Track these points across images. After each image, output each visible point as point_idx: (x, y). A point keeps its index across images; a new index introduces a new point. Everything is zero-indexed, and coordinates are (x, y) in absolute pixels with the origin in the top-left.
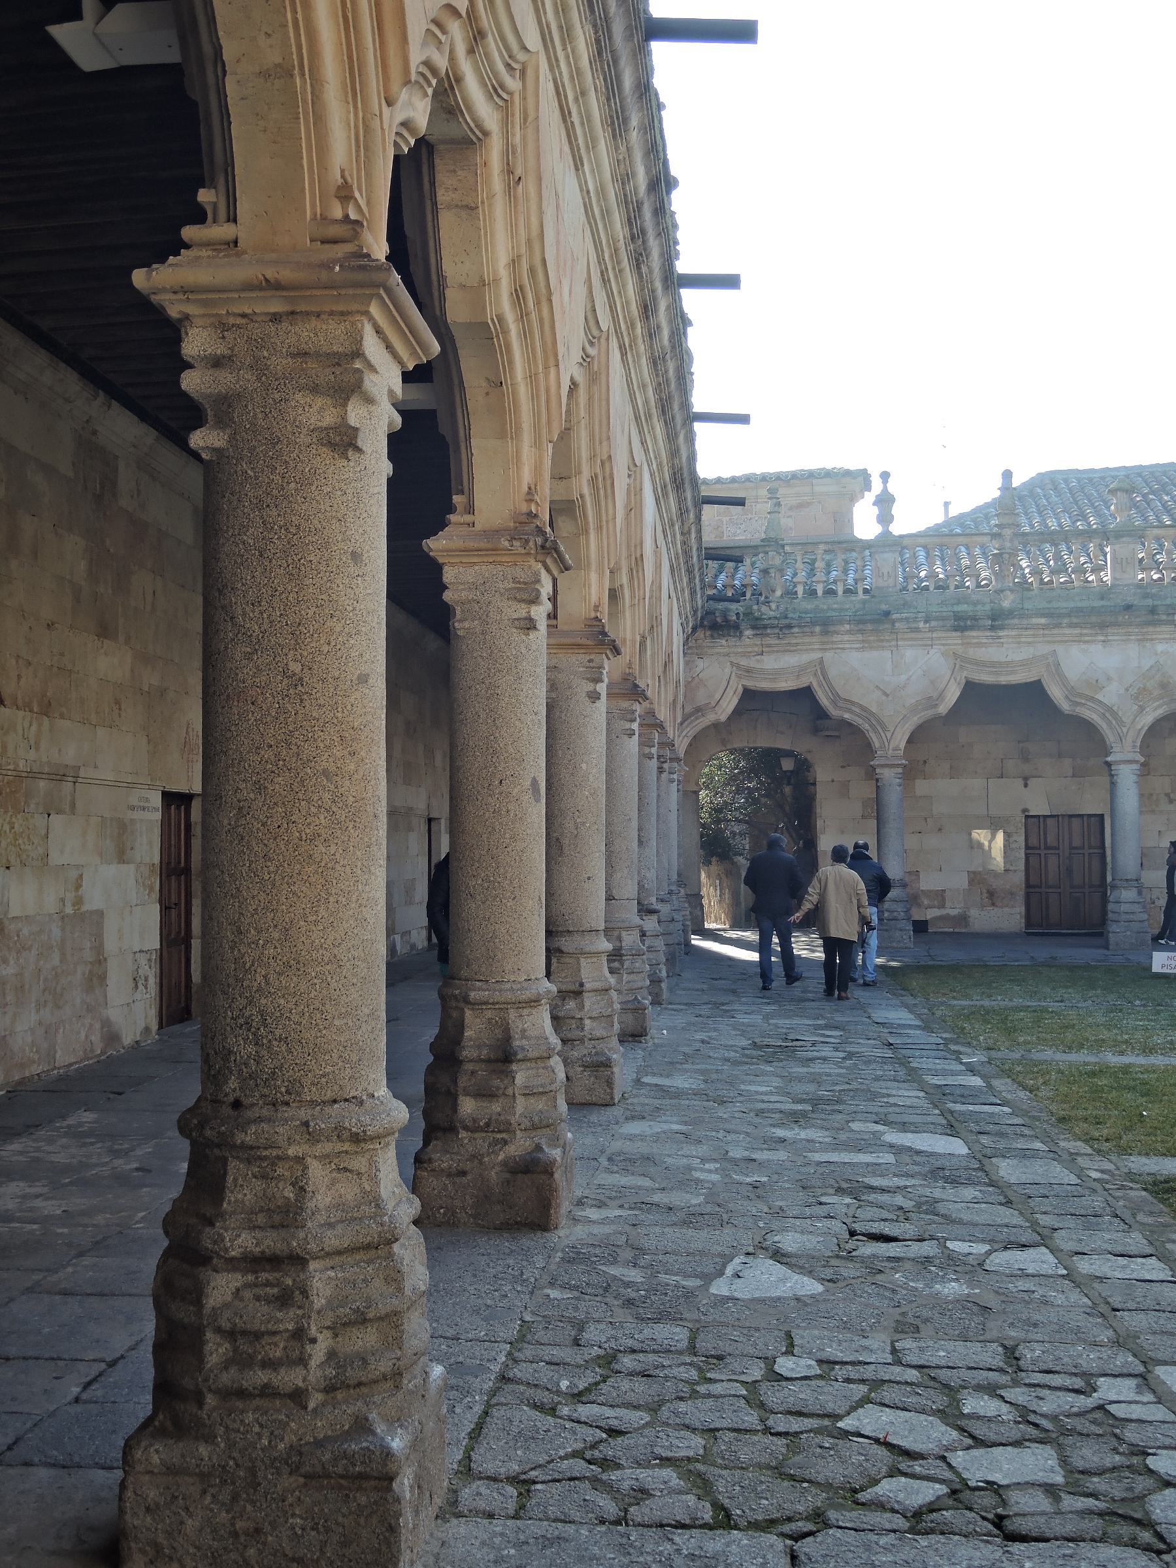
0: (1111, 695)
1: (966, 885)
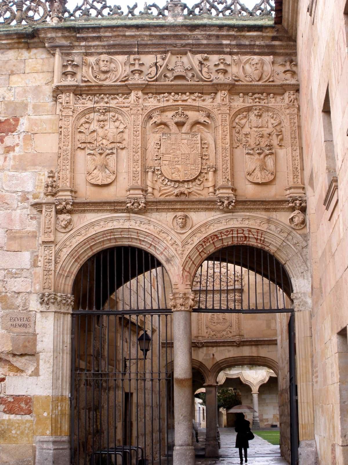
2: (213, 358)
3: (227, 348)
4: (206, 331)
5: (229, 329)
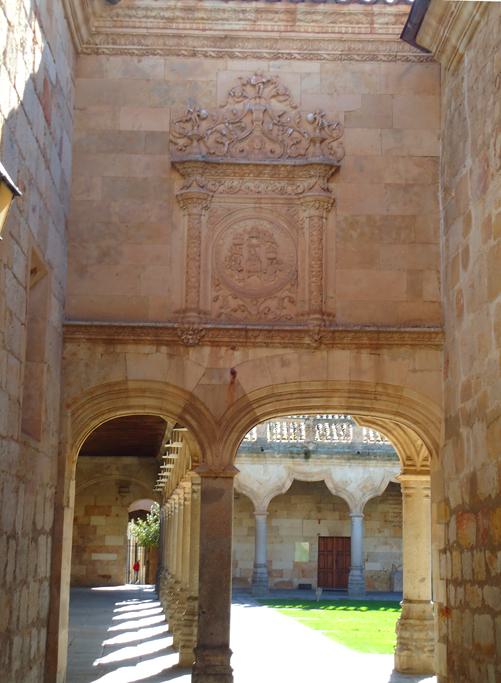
0: (351, 488)
1: (292, 567)
2: (232, 383)
3: (280, 351)
4: (211, 293)
5: (286, 293)
